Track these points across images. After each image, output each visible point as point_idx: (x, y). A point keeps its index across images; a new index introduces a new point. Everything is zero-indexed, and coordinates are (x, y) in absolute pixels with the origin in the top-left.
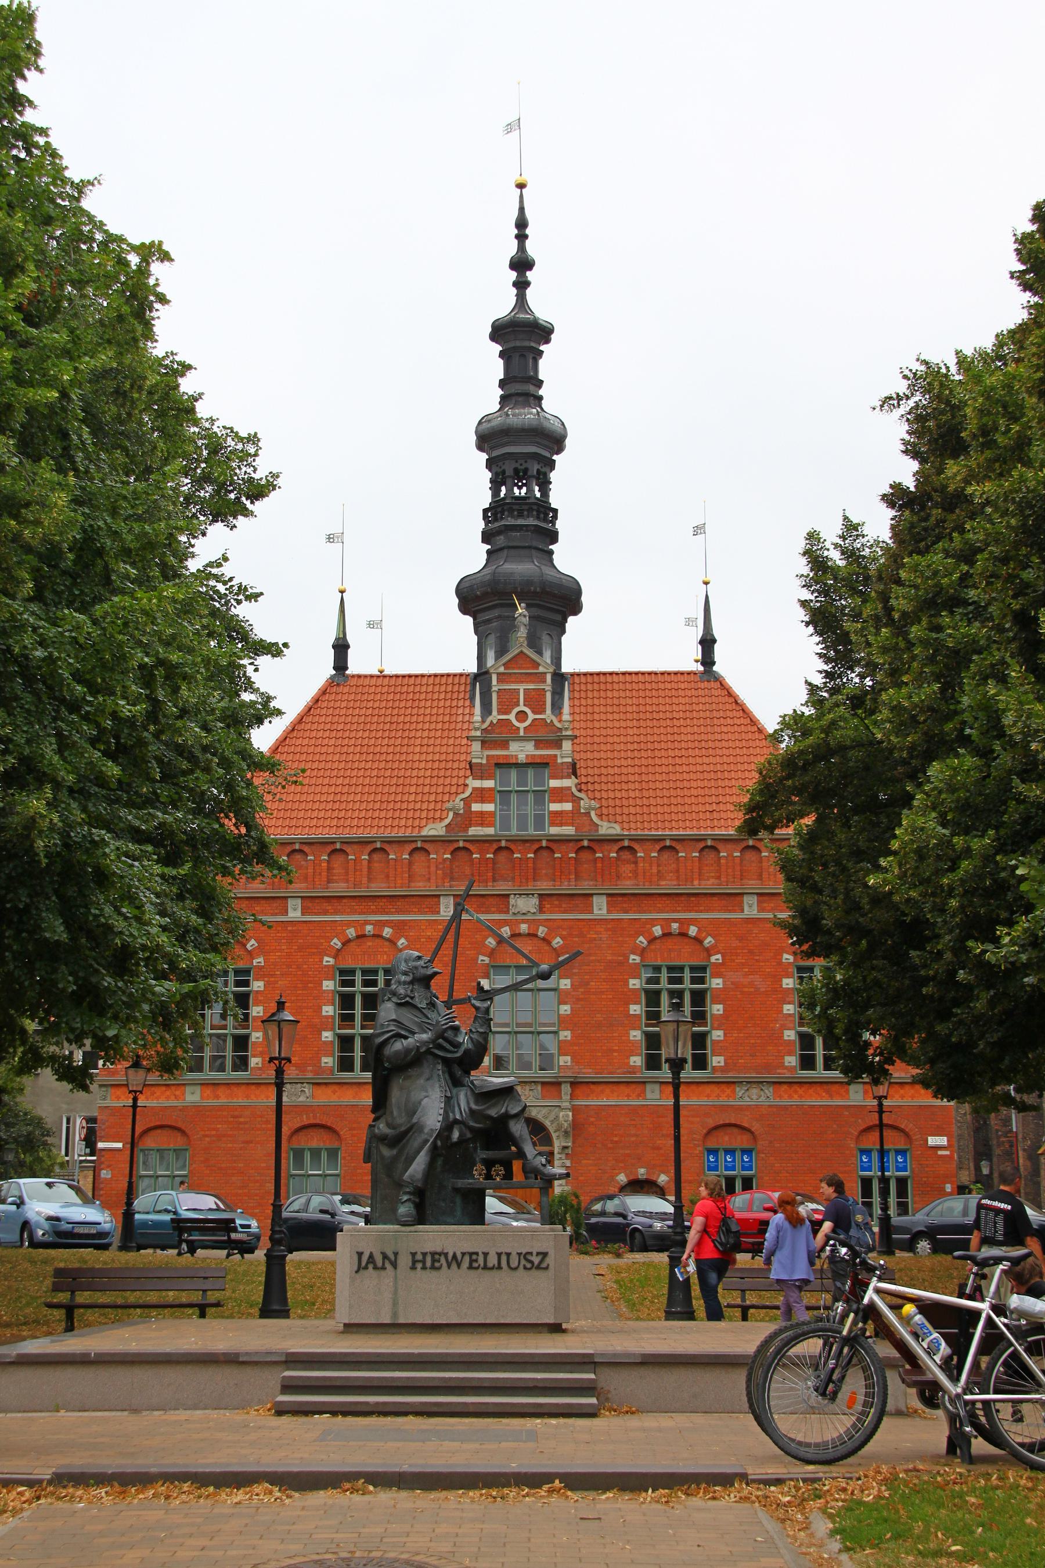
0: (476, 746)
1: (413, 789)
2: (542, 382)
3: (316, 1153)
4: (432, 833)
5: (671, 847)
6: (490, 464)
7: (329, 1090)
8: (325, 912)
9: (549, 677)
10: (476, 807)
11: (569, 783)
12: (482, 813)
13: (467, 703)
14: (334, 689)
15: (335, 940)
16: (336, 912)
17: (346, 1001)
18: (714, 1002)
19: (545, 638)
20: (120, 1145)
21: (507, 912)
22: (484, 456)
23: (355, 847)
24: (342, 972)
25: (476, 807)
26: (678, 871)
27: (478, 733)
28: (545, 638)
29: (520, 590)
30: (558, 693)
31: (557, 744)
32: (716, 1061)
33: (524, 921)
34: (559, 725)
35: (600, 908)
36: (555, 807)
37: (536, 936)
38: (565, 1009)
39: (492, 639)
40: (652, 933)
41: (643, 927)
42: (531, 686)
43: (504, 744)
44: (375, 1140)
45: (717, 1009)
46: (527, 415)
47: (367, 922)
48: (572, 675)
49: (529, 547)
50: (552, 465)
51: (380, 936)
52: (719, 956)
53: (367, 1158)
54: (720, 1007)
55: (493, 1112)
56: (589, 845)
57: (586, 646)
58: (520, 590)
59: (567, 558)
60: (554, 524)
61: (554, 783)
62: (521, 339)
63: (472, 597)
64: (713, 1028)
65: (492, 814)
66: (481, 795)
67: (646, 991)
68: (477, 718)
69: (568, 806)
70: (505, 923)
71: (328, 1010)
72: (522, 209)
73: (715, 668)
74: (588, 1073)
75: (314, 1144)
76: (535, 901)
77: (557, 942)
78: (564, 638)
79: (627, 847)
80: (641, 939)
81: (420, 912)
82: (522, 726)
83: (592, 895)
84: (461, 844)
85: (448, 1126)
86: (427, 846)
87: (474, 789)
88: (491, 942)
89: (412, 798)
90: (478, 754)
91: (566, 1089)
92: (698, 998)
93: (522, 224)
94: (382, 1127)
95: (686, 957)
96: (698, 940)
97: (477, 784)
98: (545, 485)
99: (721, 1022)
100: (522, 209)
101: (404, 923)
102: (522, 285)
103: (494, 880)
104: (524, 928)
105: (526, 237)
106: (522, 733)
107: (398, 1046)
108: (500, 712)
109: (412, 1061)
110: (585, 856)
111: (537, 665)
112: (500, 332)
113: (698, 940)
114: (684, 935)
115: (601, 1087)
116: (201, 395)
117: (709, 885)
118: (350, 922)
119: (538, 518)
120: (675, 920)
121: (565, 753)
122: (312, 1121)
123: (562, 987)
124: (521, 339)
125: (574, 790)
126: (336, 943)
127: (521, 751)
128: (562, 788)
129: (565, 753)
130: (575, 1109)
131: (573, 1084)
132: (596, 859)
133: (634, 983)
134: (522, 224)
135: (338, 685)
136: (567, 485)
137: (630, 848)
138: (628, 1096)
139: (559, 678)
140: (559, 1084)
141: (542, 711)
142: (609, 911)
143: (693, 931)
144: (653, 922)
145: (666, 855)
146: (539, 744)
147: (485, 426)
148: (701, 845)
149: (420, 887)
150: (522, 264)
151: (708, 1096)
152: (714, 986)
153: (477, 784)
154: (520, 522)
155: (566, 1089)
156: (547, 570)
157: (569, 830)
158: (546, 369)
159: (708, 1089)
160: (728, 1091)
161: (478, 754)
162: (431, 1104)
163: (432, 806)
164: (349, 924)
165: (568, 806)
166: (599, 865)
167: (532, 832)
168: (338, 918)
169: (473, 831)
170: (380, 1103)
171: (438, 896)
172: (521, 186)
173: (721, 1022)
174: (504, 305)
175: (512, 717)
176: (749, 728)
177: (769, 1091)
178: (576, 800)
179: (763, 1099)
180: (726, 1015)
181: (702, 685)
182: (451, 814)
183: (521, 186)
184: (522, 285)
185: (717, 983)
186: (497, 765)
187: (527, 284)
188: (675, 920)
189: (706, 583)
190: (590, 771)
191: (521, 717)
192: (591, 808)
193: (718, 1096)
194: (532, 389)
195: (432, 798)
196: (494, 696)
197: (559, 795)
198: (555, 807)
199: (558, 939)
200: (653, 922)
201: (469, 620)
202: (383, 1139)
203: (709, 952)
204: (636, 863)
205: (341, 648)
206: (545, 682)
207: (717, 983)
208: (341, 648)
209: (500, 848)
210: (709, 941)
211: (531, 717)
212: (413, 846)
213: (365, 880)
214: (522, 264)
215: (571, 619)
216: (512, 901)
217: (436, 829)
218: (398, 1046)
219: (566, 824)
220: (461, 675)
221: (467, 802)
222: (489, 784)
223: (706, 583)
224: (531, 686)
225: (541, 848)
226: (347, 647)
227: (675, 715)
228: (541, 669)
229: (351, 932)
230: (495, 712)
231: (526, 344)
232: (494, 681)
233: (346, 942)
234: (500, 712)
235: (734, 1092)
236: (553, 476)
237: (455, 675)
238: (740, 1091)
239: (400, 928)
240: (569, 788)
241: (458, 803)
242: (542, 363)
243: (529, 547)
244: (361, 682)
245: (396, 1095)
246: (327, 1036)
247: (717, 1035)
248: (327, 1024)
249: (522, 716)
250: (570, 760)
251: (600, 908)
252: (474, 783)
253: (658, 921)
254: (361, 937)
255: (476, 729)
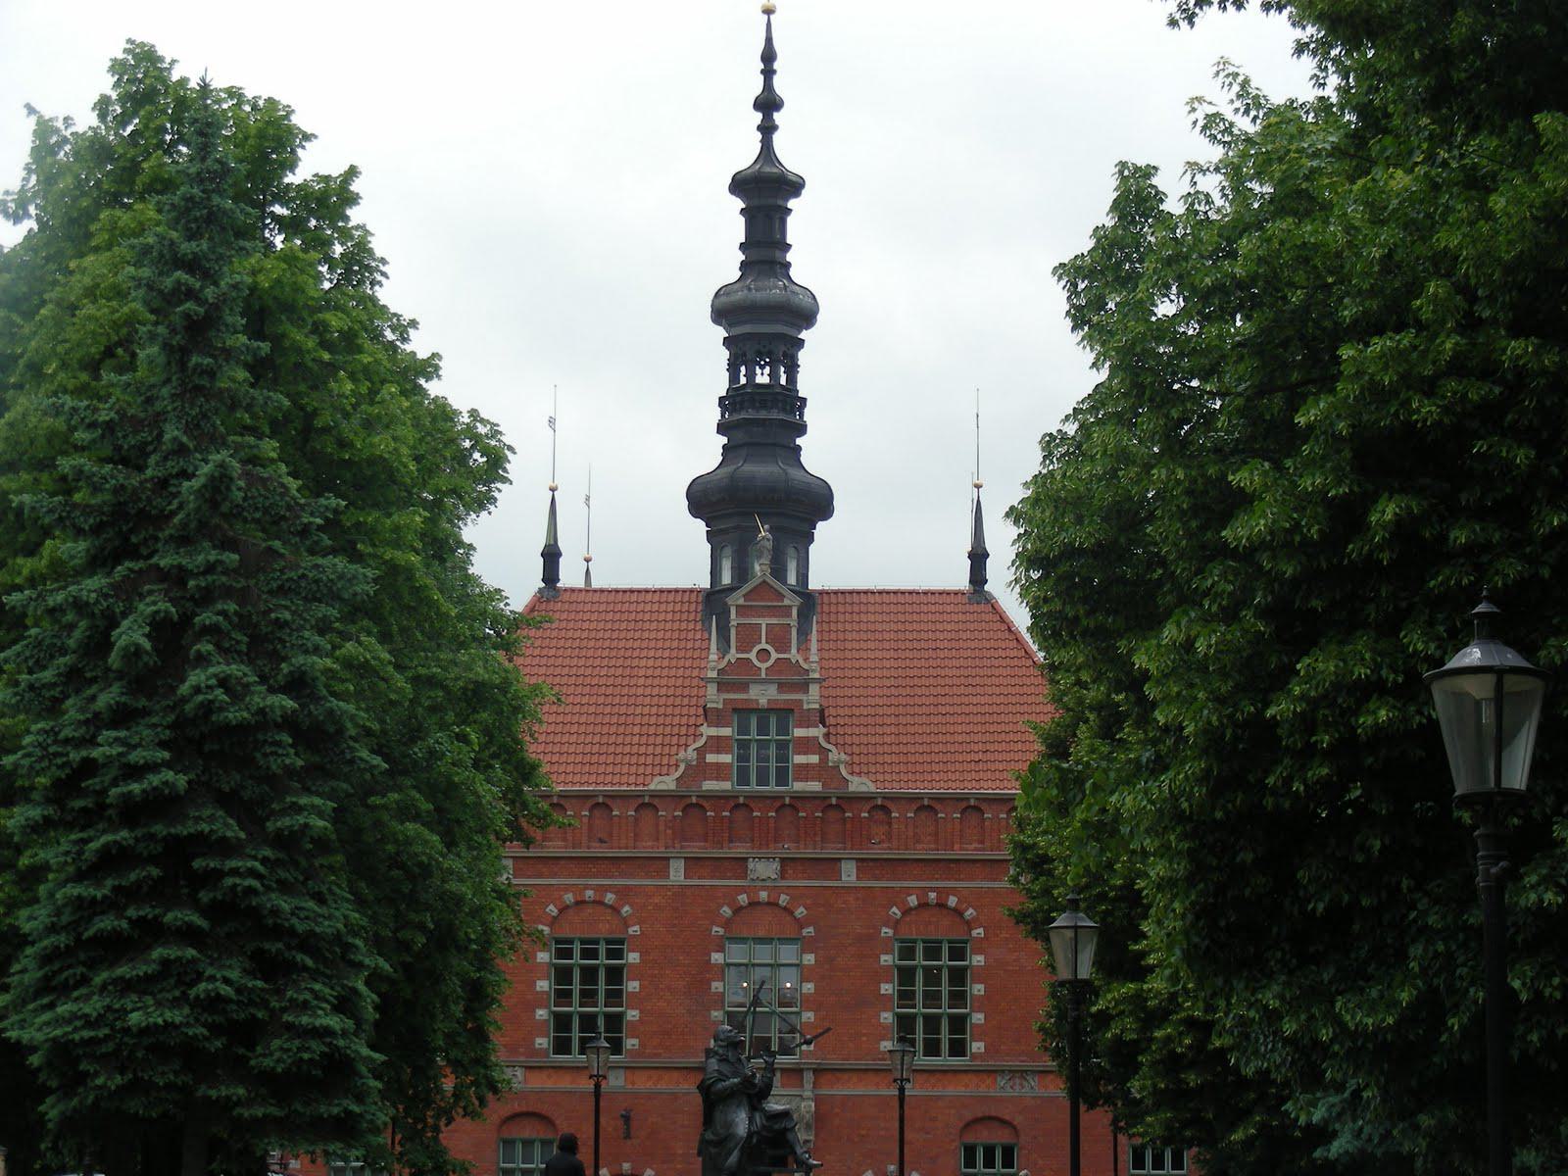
0: (712, 689)
1: (636, 730)
2: (790, 246)
3: (528, 1144)
4: (659, 787)
5: (930, 807)
6: (727, 342)
7: (544, 1075)
8: (540, 876)
9: (795, 612)
10: (711, 758)
11: (817, 732)
12: (718, 765)
13: (699, 626)
14: (544, 605)
15: (551, 907)
16: (554, 875)
17: (563, 975)
18: (973, 981)
19: (791, 551)
21: (744, 876)
22: (721, 333)
23: (574, 801)
24: (558, 941)
25: (711, 758)
26: (936, 834)
27: (714, 674)
28: (791, 551)
29: (761, 494)
30: (805, 615)
31: (804, 686)
32: (977, 1047)
33: (764, 888)
34: (806, 666)
35: (849, 874)
36: (799, 759)
37: (777, 905)
38: (809, 987)
39: (728, 551)
40: (905, 902)
41: (895, 896)
42: (774, 621)
43: (743, 687)
44: (704, 1144)
45: (978, 989)
46: (771, 291)
47: (587, 887)
48: (822, 593)
49: (774, 445)
50: (801, 343)
51: (601, 903)
52: (981, 930)
53: (699, 1154)
54: (981, 987)
55: (776, 1127)
56: (837, 805)
57: (835, 558)
58: (761, 494)
59: (817, 453)
60: (801, 415)
61: (799, 732)
62: (765, 193)
63: (703, 499)
64: (972, 1011)
65: (729, 766)
66: (717, 744)
67: (900, 969)
68: (713, 657)
69: (814, 759)
70: (743, 890)
71: (543, 985)
72: (769, 40)
73: (986, 588)
74: (834, 1061)
75: (527, 1134)
76: (776, 865)
77: (800, 912)
78: (812, 548)
79: (881, 806)
80: (894, 909)
81: (648, 876)
82: (764, 666)
83: (839, 860)
84: (694, 800)
85: (750, 1135)
86: (656, 802)
87: (710, 738)
88: (726, 911)
89: (636, 739)
90: (714, 697)
91: (808, 1077)
92: (958, 976)
93: (768, 56)
94: (709, 1136)
95: (942, 930)
96: (958, 912)
97: (713, 731)
98: (792, 369)
99: (981, 1004)
100: (769, 40)
101: (628, 888)
102: (767, 129)
103: (731, 841)
104: (763, 895)
105: (774, 72)
106: (763, 676)
107: (720, 1085)
108: (739, 650)
109: (730, 1096)
110: (832, 815)
111: (781, 597)
112: (740, 185)
113: (958, 912)
114: (941, 905)
115: (846, 1076)
116: (352, 172)
117: (970, 851)
118: (569, 887)
119: (784, 410)
120: (932, 889)
121: (812, 698)
122: (524, 1109)
123: (805, 962)
124: (765, 193)
125: (822, 741)
126: (552, 910)
127: (763, 695)
128: (807, 738)
129: (812, 698)
130: (817, 1099)
131: (815, 1071)
132: (844, 820)
133: (886, 959)
134: (768, 56)
135: (548, 601)
136: (818, 366)
137: (883, 807)
138: (877, 1085)
139: (810, 601)
140: (801, 1071)
141: (787, 650)
142: (858, 878)
143: (952, 901)
144: (908, 891)
145: (923, 815)
146: (782, 687)
147: (723, 299)
148: (964, 804)
149: (647, 848)
150: (768, 104)
151: (966, 1086)
152: (975, 963)
153: (713, 731)
154: (763, 415)
155: (808, 1077)
156: (794, 472)
157: (815, 786)
158: (797, 228)
159: (966, 1078)
160: (989, 1081)
161: (714, 697)
162: (741, 1122)
163: (658, 750)
164: (567, 888)
165: (814, 759)
166: (848, 826)
167: (772, 788)
168: (553, 881)
169: (709, 785)
170: (708, 1120)
171: (668, 859)
172: (768, 11)
173: (981, 1004)
174: (745, 153)
175: (752, 656)
176: (1024, 662)
177: (1033, 1081)
178: (823, 752)
179: (1027, 1089)
180: (988, 996)
181: (972, 608)
182: (682, 767)
183: (768, 11)
184: (767, 129)
185: (978, 960)
186: (735, 710)
187: (775, 128)
188: (932, 889)
189: (978, 487)
190: (841, 712)
191: (762, 657)
192: (840, 761)
193: (978, 1086)
194: (778, 254)
195: (659, 740)
196: (733, 632)
197: (807, 745)
198: (799, 759)
199: (802, 909)
200: (908, 891)
201: (700, 527)
202: (709, 1142)
203: (970, 925)
204: (890, 824)
205: (551, 556)
206: (789, 615)
207: (978, 960)
208: (551, 556)
209: (737, 806)
210: (970, 913)
211: (774, 655)
212: (640, 801)
213: (585, 839)
214: (768, 104)
215: (820, 525)
216: (751, 865)
217: (667, 783)
218: (720, 1085)
219: (813, 780)
220: (692, 591)
221: (701, 752)
222: (726, 732)
223: (978, 487)
224: (774, 621)
225: (784, 805)
226: (559, 554)
227: (938, 644)
228: (787, 602)
229: (569, 898)
230: (733, 650)
231: (771, 201)
232: (733, 615)
233: (563, 909)
234: (739, 650)
235: (995, 1082)
236: (803, 356)
237: (684, 591)
238: (1001, 1082)
239: (624, 893)
240: (816, 738)
241: (690, 754)
242: (790, 221)
243: (774, 445)
244: (574, 597)
245: (718, 1116)
246: (541, 1014)
247: (978, 1018)
248: (540, 1001)
249: (764, 654)
250: (817, 706)
251: (849, 874)
252: (709, 731)
253: (914, 890)
254: (580, 903)
255: (713, 669)
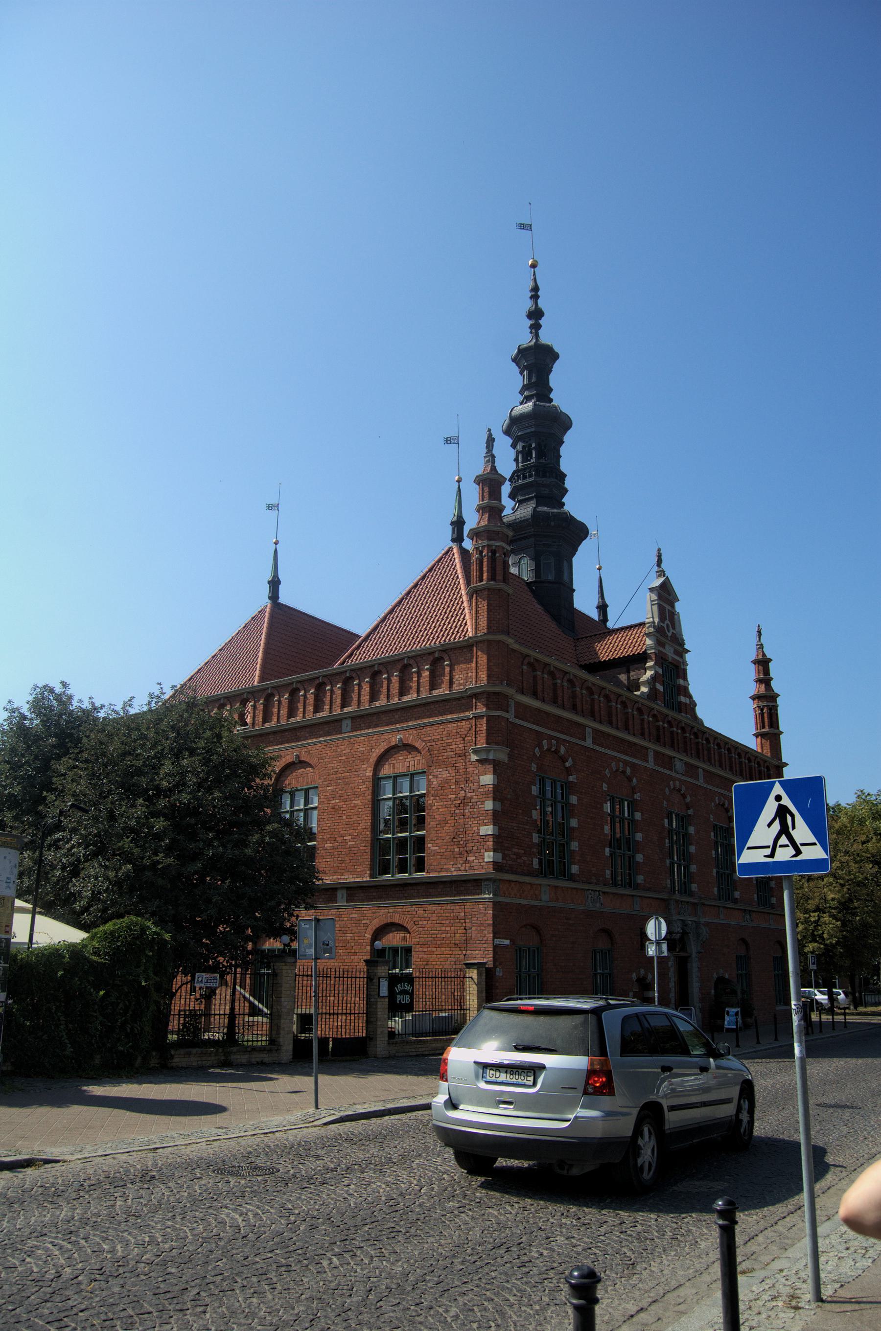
20: (507, 942)
47: (620, 760)
62: (537, 362)
102: (536, 328)
124: (537, 362)
127: (669, 651)
150: (536, 315)
168: (609, 752)
175: (665, 625)
184: (536, 328)
214: (536, 315)
